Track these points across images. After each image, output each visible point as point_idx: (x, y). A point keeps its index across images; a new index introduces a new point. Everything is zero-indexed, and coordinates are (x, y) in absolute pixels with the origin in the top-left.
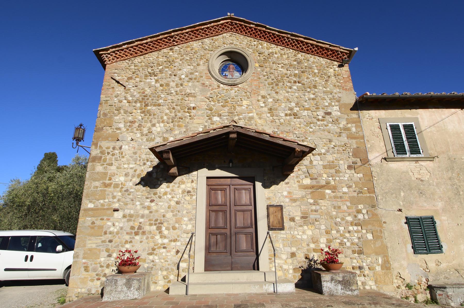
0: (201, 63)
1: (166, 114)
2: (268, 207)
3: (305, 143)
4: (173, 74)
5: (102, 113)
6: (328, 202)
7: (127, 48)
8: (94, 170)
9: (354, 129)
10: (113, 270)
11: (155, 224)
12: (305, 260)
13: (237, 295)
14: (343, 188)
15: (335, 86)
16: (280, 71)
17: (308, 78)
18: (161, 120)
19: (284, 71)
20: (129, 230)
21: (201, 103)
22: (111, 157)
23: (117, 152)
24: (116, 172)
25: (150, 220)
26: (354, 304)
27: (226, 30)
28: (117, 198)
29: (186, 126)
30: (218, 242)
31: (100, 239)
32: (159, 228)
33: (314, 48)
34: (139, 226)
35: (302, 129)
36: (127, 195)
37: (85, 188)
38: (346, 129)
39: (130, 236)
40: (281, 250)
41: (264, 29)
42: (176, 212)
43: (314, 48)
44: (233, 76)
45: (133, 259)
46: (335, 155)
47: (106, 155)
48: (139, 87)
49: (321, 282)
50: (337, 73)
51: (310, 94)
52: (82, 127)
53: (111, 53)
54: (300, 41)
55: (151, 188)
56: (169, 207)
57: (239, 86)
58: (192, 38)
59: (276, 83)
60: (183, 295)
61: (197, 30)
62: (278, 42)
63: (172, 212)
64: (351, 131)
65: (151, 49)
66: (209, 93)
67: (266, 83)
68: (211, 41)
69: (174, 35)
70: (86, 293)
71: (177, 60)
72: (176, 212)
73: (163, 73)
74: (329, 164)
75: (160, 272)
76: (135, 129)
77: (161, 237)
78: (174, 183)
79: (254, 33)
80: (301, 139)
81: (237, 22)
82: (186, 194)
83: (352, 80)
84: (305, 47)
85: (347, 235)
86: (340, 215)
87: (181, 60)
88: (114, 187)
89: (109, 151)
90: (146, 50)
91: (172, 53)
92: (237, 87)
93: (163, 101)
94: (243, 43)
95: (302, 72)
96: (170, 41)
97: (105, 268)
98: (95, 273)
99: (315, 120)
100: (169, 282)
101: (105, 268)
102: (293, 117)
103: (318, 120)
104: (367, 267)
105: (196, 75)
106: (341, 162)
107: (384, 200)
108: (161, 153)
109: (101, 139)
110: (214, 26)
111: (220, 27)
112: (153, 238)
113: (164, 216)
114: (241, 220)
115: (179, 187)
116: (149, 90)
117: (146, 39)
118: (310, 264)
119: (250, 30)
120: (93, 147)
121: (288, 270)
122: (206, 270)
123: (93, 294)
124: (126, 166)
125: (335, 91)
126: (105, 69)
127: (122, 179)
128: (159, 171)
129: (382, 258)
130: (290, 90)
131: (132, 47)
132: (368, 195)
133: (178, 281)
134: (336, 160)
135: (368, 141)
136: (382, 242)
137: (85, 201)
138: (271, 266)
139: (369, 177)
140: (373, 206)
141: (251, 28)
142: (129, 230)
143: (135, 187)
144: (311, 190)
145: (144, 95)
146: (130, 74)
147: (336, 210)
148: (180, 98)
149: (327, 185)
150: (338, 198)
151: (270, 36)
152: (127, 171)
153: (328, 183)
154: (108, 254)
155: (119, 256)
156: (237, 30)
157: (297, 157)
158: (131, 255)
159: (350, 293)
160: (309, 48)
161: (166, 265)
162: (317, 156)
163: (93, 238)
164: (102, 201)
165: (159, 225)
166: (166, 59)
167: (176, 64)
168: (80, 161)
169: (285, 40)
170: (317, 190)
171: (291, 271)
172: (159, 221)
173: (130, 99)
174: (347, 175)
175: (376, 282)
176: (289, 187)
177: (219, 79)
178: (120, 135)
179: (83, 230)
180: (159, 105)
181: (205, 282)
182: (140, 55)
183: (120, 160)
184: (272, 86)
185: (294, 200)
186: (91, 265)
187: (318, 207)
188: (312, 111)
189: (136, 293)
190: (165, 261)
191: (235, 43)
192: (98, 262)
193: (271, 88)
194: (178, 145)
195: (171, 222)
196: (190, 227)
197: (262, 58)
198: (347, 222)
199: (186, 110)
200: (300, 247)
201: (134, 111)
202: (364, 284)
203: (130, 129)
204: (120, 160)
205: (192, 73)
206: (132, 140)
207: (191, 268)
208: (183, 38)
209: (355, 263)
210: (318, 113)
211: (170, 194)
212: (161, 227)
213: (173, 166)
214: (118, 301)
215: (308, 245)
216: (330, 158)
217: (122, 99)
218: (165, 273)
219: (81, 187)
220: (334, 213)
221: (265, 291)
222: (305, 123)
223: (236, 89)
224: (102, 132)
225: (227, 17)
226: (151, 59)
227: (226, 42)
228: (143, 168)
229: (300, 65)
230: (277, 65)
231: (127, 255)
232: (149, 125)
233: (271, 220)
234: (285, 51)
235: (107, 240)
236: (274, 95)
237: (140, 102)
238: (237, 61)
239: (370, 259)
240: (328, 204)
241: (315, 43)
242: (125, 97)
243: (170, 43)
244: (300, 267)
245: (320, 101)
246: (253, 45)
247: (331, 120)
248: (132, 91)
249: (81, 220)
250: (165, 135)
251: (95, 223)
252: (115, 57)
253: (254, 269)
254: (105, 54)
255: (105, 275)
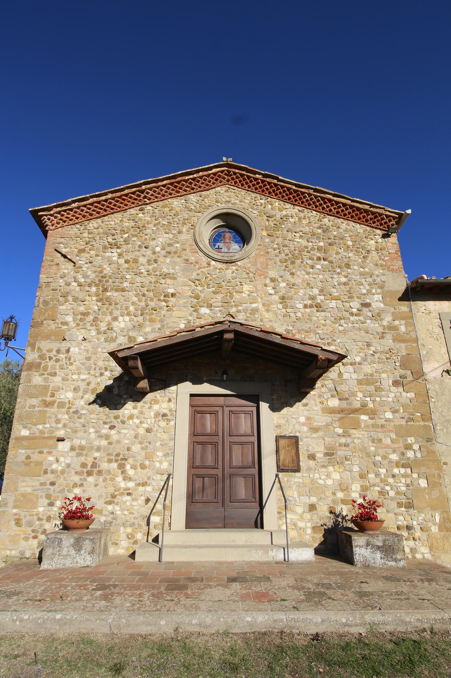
0: (184, 230)
1: (133, 304)
2: (278, 439)
3: (332, 348)
4: (144, 245)
5: (41, 300)
6: (364, 432)
7: (78, 208)
8: (30, 382)
9: (403, 329)
10: (55, 525)
11: (116, 461)
12: (329, 515)
13: (232, 563)
14: (386, 414)
15: (377, 265)
16: (298, 242)
17: (337, 253)
18: (126, 312)
19: (304, 242)
20: (79, 469)
21: (184, 288)
22: (54, 363)
23: (62, 356)
24: (61, 385)
25: (109, 455)
26: (399, 580)
27: (221, 182)
28: (63, 422)
29: (161, 321)
30: (205, 487)
31: (38, 480)
32: (121, 467)
33: (347, 209)
34: (94, 462)
35: (328, 327)
36: (76, 418)
37: (17, 407)
38: (392, 328)
39: (80, 477)
40: (295, 501)
41: (275, 181)
42: (145, 444)
43: (347, 209)
44: (229, 249)
45: (85, 509)
46: (375, 365)
47: (48, 360)
48: (94, 263)
49: (352, 547)
50: (380, 247)
51: (341, 276)
52: (13, 321)
53: (55, 215)
54: (327, 199)
55: (110, 409)
56: (136, 437)
57: (239, 263)
58: (171, 194)
59: (292, 260)
60: (154, 562)
61: (179, 182)
62: (296, 201)
63: (141, 443)
64: (398, 330)
65: (112, 209)
66: (195, 274)
67: (278, 259)
68: (199, 198)
69: (146, 189)
70: (17, 557)
71: (150, 226)
72: (145, 444)
73: (129, 244)
74: (365, 377)
75: (122, 528)
76: (89, 324)
77: (124, 479)
78: (144, 403)
79: (260, 187)
80: (327, 341)
81: (237, 171)
82: (160, 418)
83: (402, 257)
84: (335, 209)
85: (391, 480)
86: (381, 451)
87: (155, 226)
88: (58, 407)
89: (51, 354)
90: (105, 210)
91: (142, 215)
92: (235, 266)
93: (128, 285)
94: (245, 201)
95: (330, 244)
96: (139, 198)
97: (44, 522)
98: (31, 529)
99: (347, 315)
100: (135, 542)
101: (44, 522)
102: (315, 309)
103: (352, 314)
104: (419, 527)
105: (177, 247)
106: (384, 375)
107: (445, 431)
108: (126, 359)
109: (39, 338)
110: (203, 176)
111: (212, 178)
112: (112, 479)
113: (129, 449)
114: (238, 456)
115: (150, 408)
116: (109, 269)
117: (106, 194)
118: (337, 521)
119: (255, 183)
120: (29, 349)
121: (304, 530)
122: (188, 526)
123: (28, 559)
124: (75, 377)
125: (377, 272)
126: (46, 237)
127: (70, 395)
128: (122, 384)
129: (440, 515)
130: (311, 270)
131: (85, 206)
132: (422, 423)
133: (147, 541)
134: (376, 372)
135: (424, 346)
136: (441, 492)
137: (18, 426)
138: (281, 522)
139: (424, 397)
140: (429, 440)
141: (256, 179)
142: (79, 469)
143: (88, 407)
144: (339, 416)
145: (101, 275)
146: (81, 245)
147: (374, 445)
148: (153, 280)
149: (363, 409)
150: (378, 427)
151: (284, 191)
152: (76, 384)
153: (364, 405)
154: (48, 501)
155: (64, 505)
156: (236, 183)
157: (320, 368)
158: (82, 504)
159: (393, 563)
160: (340, 210)
161: (130, 518)
162: (349, 366)
163: (28, 479)
164: (40, 427)
165: (121, 462)
166: (134, 224)
167: (148, 231)
168: (10, 367)
169: (305, 197)
170: (347, 415)
171: (309, 531)
172: (121, 456)
173: (82, 280)
174: (392, 394)
175: (431, 548)
176: (307, 410)
177: (210, 254)
178: (68, 333)
179: (14, 468)
180: (123, 290)
181: (185, 544)
182: (97, 218)
183: (67, 368)
184: (285, 264)
185: (315, 430)
186: (25, 516)
187: (349, 440)
188: (343, 302)
189: (89, 558)
190: (130, 513)
191: (233, 202)
192: (34, 513)
193: (284, 267)
194: (150, 348)
195: (139, 458)
196: (165, 465)
197: (272, 224)
198: (391, 461)
199: (162, 298)
200: (322, 496)
201: (87, 298)
202: (413, 551)
203: (81, 324)
204: (67, 368)
205: (170, 245)
206: (85, 339)
207: (166, 524)
208: (159, 194)
209: (401, 521)
210: (351, 304)
211: (137, 418)
212: (124, 464)
213: (143, 378)
214: (63, 569)
215: (334, 494)
216: (367, 369)
217: (70, 280)
218: (129, 530)
219: (11, 405)
220: (373, 449)
221: (272, 559)
222: (333, 319)
223: (234, 268)
224: (42, 328)
225: (222, 163)
226: (113, 223)
227: (220, 200)
228: (99, 380)
229: (326, 234)
230: (294, 234)
231: (76, 504)
232: (109, 318)
233: (282, 457)
234: (306, 213)
235: (48, 483)
236: (289, 277)
237: (96, 285)
238: (235, 227)
239: (423, 515)
240: (363, 435)
241: (348, 202)
242: (75, 278)
243: (140, 200)
244: (322, 526)
245: (355, 287)
246: (260, 204)
247: (370, 314)
248: (84, 269)
249: (11, 453)
250: (131, 334)
251: (30, 458)
252: (61, 219)
253: (256, 527)
254: (46, 215)
255: (44, 532)
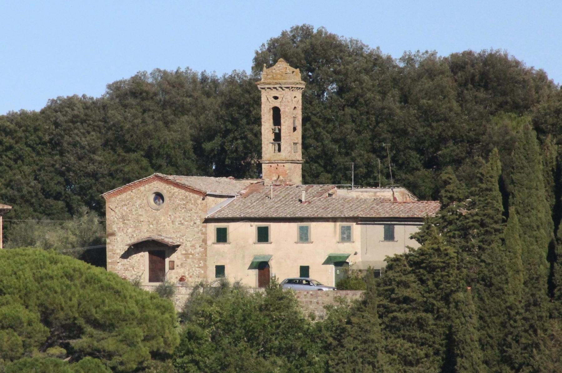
32: (133, 269)
139: (206, 249)
170: (187, 255)
216: (193, 242)
238: (159, 196)
